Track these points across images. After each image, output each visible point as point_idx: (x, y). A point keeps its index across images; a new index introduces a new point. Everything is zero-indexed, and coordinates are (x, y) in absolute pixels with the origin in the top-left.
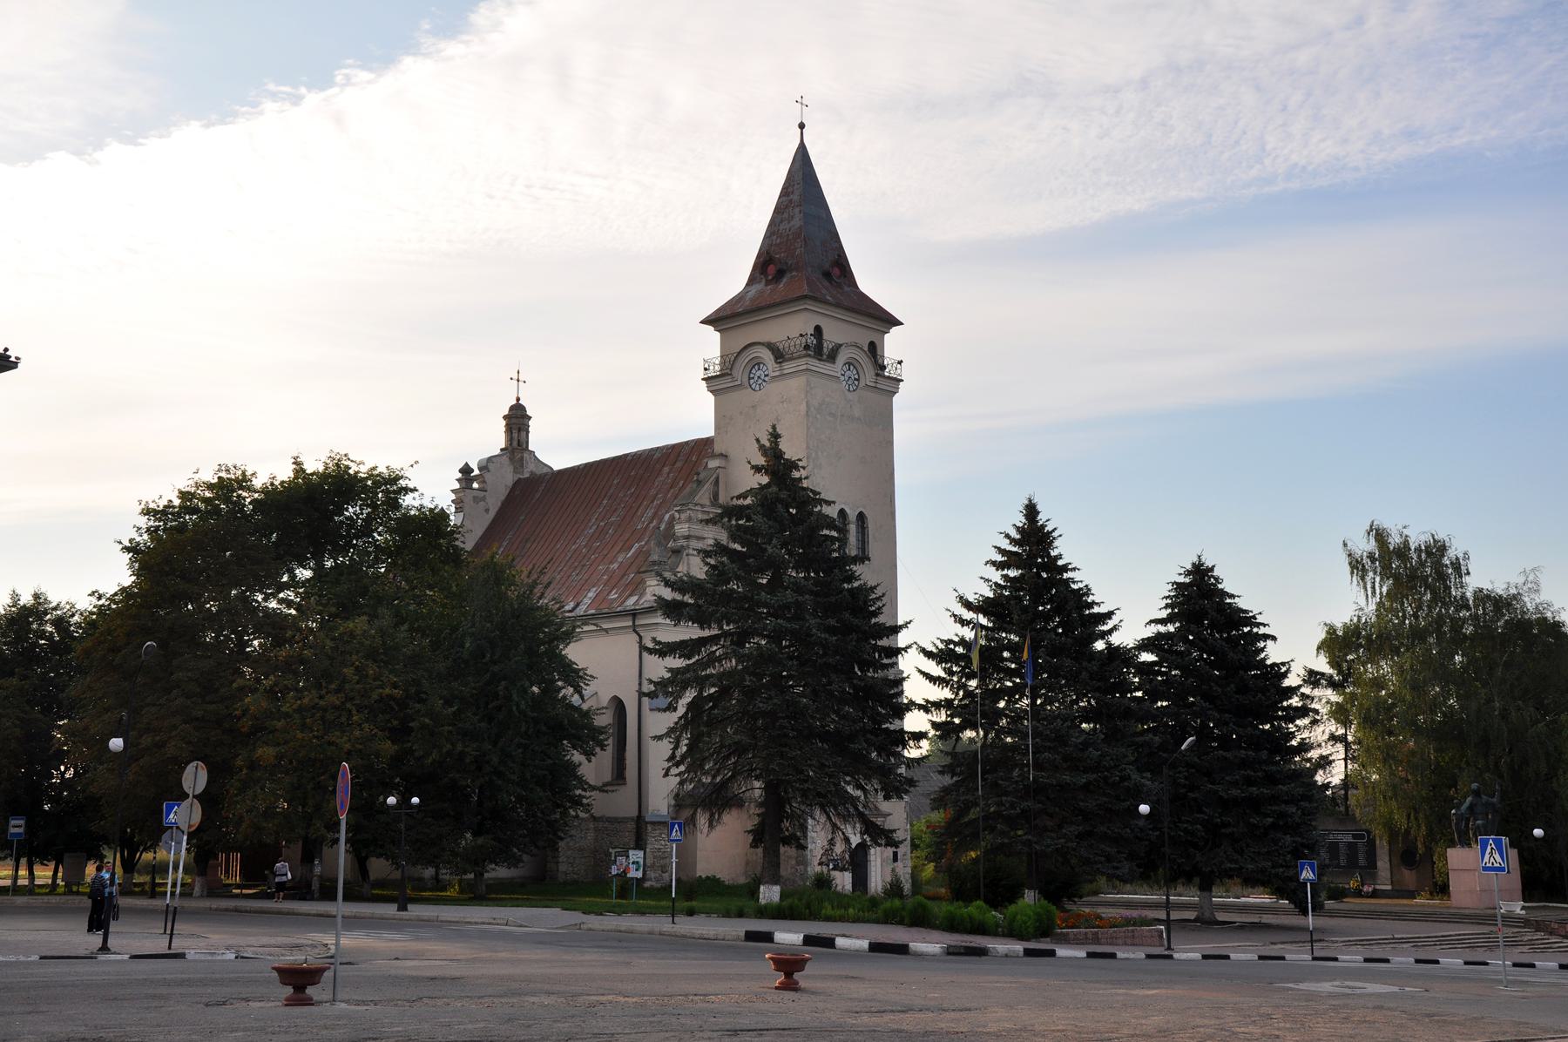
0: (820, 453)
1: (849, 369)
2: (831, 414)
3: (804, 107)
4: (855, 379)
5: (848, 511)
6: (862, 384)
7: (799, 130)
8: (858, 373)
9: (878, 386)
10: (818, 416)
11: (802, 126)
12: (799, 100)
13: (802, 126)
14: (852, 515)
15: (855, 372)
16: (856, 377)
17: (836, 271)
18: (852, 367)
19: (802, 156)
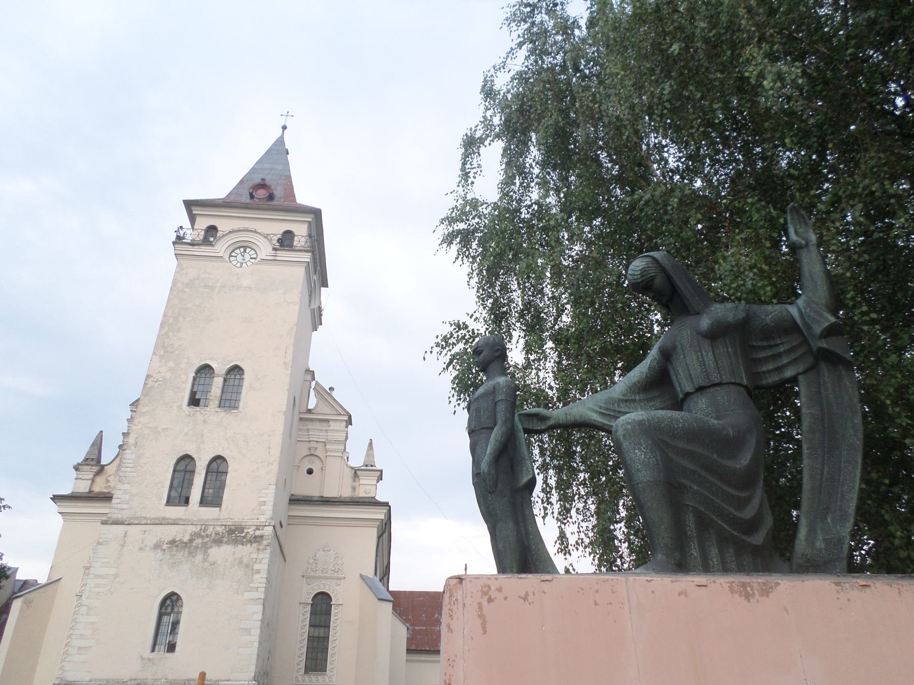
0: (181, 319)
1: (245, 251)
2: (206, 286)
3: (289, 114)
4: (251, 258)
5: (214, 365)
6: (258, 259)
7: (281, 130)
8: (256, 253)
9: (278, 258)
10: (187, 290)
11: (284, 128)
12: (286, 114)
13: (284, 128)
14: (220, 368)
15: (253, 252)
16: (255, 256)
17: (262, 193)
18: (248, 250)
19: (280, 142)
